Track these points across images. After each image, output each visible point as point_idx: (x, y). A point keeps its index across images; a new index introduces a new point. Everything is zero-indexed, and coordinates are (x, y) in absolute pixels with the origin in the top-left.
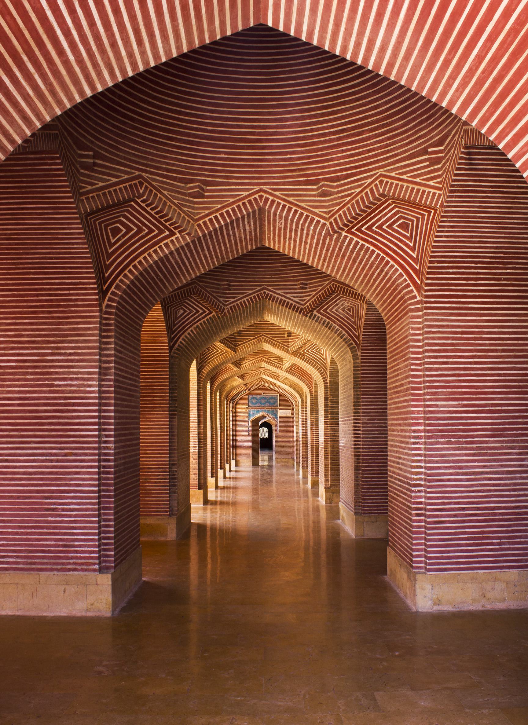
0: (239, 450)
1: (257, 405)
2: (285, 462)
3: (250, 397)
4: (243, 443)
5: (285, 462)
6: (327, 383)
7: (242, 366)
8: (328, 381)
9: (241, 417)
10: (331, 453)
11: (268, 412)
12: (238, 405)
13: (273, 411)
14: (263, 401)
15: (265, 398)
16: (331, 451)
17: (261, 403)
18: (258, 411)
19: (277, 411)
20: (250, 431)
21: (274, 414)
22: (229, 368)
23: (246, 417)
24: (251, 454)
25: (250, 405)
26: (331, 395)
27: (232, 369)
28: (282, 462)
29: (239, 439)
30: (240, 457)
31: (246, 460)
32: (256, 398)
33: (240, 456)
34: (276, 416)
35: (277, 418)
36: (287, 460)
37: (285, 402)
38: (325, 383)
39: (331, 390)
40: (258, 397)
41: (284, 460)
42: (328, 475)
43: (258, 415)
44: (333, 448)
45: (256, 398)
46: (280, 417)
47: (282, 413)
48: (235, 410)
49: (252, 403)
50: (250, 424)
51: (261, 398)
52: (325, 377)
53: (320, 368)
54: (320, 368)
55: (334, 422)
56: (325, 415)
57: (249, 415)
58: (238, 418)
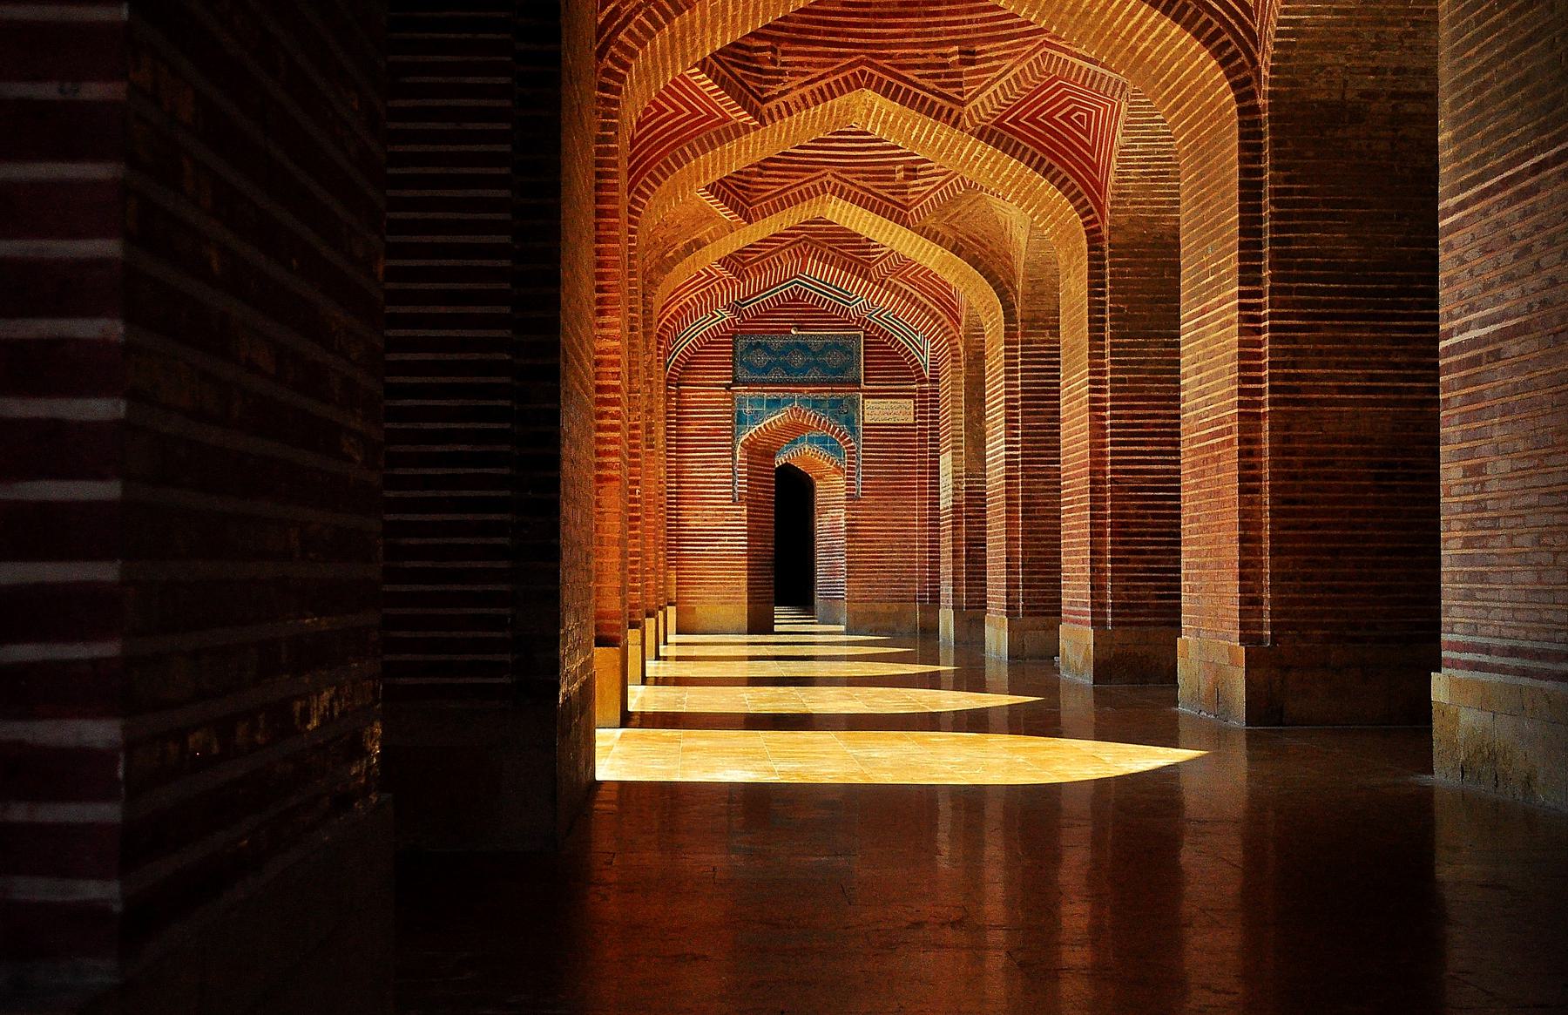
6: (1255, 109)
7: (772, 105)
8: (1261, 101)
10: (1274, 464)
11: (816, 404)
14: (798, 360)
15: (803, 348)
16: (1273, 452)
17: (787, 368)
18: (775, 404)
19: (854, 403)
20: (742, 486)
21: (845, 413)
22: (711, 115)
26: (1274, 167)
27: (726, 119)
29: (695, 519)
32: (767, 349)
33: (699, 592)
34: (850, 422)
35: (853, 430)
37: (890, 364)
38: (1248, 112)
39: (1275, 143)
42: (1259, 577)
43: (776, 418)
44: (1287, 439)
45: (767, 349)
49: (750, 367)
51: (788, 349)
52: (1248, 81)
53: (1218, 33)
54: (1218, 33)
55: (1294, 304)
56: (1242, 269)
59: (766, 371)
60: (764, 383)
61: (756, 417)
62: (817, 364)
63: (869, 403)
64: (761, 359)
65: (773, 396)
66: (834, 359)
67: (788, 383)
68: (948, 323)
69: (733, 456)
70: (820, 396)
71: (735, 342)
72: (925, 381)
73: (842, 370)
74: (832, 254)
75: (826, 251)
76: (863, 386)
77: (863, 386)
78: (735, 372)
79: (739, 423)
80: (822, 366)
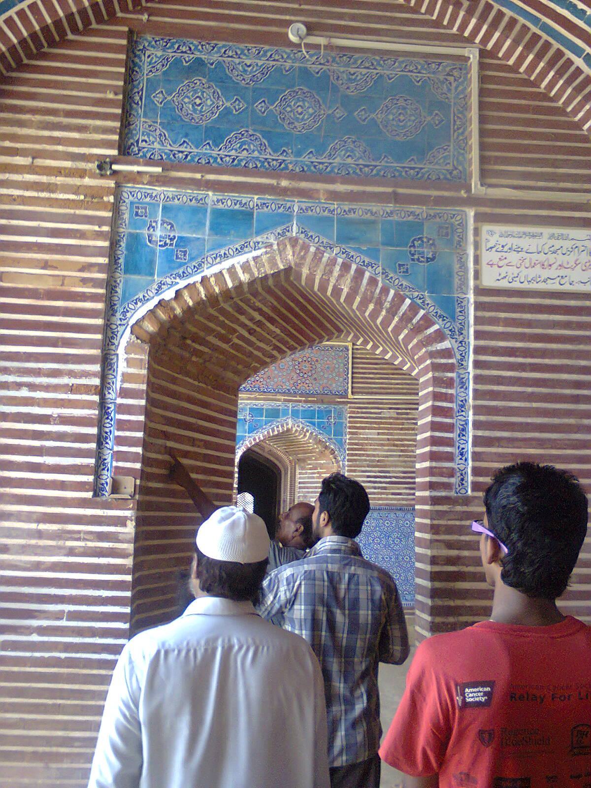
11: (349, 233)
13: (405, 235)
14: (303, 113)
15: (319, 84)
17: (275, 138)
18: (234, 223)
19: (452, 235)
20: (126, 453)
23: (80, 269)
25: (149, 135)
32: (221, 79)
34: (441, 283)
35: (451, 308)
40: (248, 61)
43: (235, 265)
46: (494, 301)
49: (174, 121)
50: (130, 364)
57: (123, 258)
59: (215, 135)
61: (180, 254)
64: (202, 102)
65: (230, 201)
67: (275, 172)
69: (107, 361)
70: (360, 211)
71: (132, 49)
79: (132, 268)
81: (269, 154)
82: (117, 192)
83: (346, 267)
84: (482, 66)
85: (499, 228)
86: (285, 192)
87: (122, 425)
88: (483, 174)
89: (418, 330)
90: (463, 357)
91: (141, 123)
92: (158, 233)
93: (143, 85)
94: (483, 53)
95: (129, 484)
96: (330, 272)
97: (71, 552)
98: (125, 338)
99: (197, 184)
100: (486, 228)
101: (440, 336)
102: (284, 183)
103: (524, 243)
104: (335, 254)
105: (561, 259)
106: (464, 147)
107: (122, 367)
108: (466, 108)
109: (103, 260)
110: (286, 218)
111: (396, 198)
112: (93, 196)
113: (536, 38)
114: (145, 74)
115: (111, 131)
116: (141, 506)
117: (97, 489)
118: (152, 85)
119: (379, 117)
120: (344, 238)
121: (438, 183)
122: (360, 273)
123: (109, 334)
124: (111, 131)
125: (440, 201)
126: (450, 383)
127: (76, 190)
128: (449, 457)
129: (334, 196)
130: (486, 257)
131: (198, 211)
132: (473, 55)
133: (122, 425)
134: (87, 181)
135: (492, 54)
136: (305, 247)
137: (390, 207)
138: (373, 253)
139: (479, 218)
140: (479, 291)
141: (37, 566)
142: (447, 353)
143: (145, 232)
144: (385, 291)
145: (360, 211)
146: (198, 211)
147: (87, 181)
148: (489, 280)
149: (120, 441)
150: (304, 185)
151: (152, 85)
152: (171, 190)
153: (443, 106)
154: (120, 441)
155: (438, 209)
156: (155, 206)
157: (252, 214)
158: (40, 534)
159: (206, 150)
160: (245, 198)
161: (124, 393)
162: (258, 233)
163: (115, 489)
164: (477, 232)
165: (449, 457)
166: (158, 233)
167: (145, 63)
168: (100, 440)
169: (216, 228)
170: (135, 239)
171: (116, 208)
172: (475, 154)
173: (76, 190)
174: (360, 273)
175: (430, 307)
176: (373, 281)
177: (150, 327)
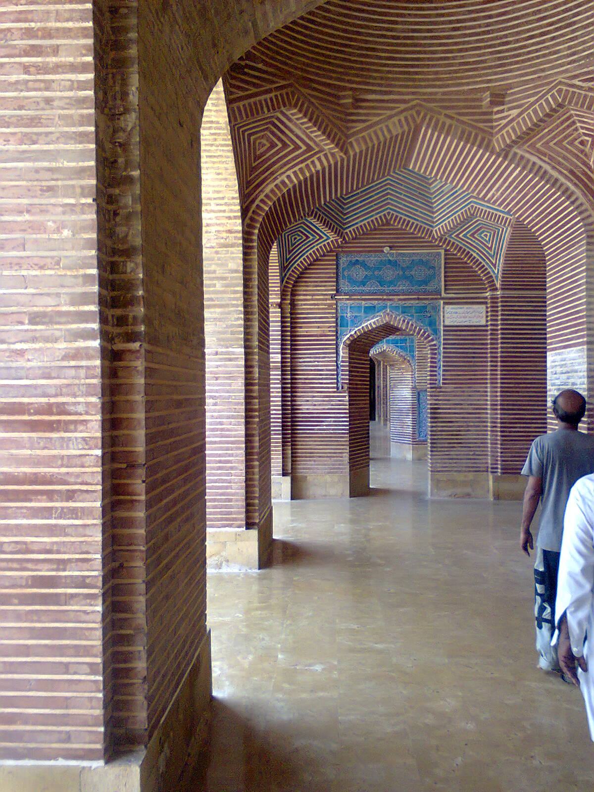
0: (306, 444)
1: (366, 289)
2: (465, 483)
3: (343, 260)
4: (318, 419)
5: (465, 483)
9: (314, 330)
11: (405, 310)
12: (301, 289)
13: (422, 310)
14: (389, 274)
15: (394, 264)
19: (436, 309)
20: (344, 377)
23: (328, 328)
24: (346, 457)
25: (345, 286)
28: (453, 483)
29: (307, 404)
30: (306, 467)
31: (328, 478)
32: (364, 265)
33: (310, 464)
34: (433, 324)
35: (436, 331)
36: (471, 476)
40: (372, 259)
41: (460, 477)
43: (371, 322)
45: (364, 265)
46: (449, 329)
47: (454, 315)
48: (293, 305)
49: (352, 281)
50: (343, 353)
57: (340, 323)
58: (301, 331)
59: (363, 284)
60: (361, 294)
61: (356, 321)
62: (407, 278)
63: (449, 308)
64: (359, 273)
66: (418, 273)
68: (582, 199)
69: (337, 353)
70: (408, 303)
71: (337, 260)
72: (496, 289)
73: (425, 282)
74: (448, 122)
75: (442, 119)
76: (443, 295)
77: (443, 295)
78: (337, 285)
80: (410, 279)
81: (380, 288)
82: (336, 304)
83: (404, 321)
84: (446, 255)
85: (451, 306)
86: (385, 299)
87: (343, 371)
88: (446, 289)
89: (426, 338)
90: (440, 346)
91: (341, 281)
92: (349, 315)
93: (341, 270)
94: (446, 250)
95: (346, 386)
96: (398, 320)
97: (332, 405)
98: (341, 346)
99: (358, 299)
100: (446, 306)
101: (432, 340)
102: (385, 297)
103: (459, 311)
104: (401, 317)
105: (469, 315)
106: (440, 281)
107: (341, 354)
108: (440, 268)
109: (334, 325)
110: (385, 307)
111: (418, 299)
112: (330, 305)
113: (461, 248)
114: (341, 267)
115: (334, 286)
116: (349, 392)
117: (338, 388)
118: (344, 269)
119: (413, 273)
120: (403, 312)
121: (430, 293)
122: (408, 323)
123: (337, 345)
124: (334, 286)
125: (432, 299)
126: (435, 354)
127: (325, 305)
128: (435, 375)
129: (400, 300)
130: (446, 315)
131: (360, 307)
132: (443, 252)
133: (343, 371)
134: (328, 302)
135: (449, 250)
136: (392, 316)
137: (417, 302)
138: (412, 316)
139: (444, 303)
140: (444, 326)
141: (324, 409)
142: (435, 345)
143: (345, 315)
144: (416, 328)
145: (408, 303)
146: (360, 307)
147: (328, 302)
148: (447, 323)
149: (342, 375)
150: (391, 297)
151: (344, 269)
152: (351, 302)
153: (433, 268)
154: (342, 375)
155: (432, 301)
156: (347, 307)
157: (374, 307)
158: (324, 401)
159: (360, 288)
160: (373, 302)
161: (343, 362)
162: (378, 312)
163: (342, 388)
164: (443, 308)
165: (435, 375)
166: (349, 315)
167: (341, 261)
168: (337, 375)
169: (365, 312)
170: (342, 317)
171: (336, 309)
172: (443, 283)
173: (325, 305)
174: (408, 323)
175: (430, 331)
176: (412, 325)
177: (348, 342)
